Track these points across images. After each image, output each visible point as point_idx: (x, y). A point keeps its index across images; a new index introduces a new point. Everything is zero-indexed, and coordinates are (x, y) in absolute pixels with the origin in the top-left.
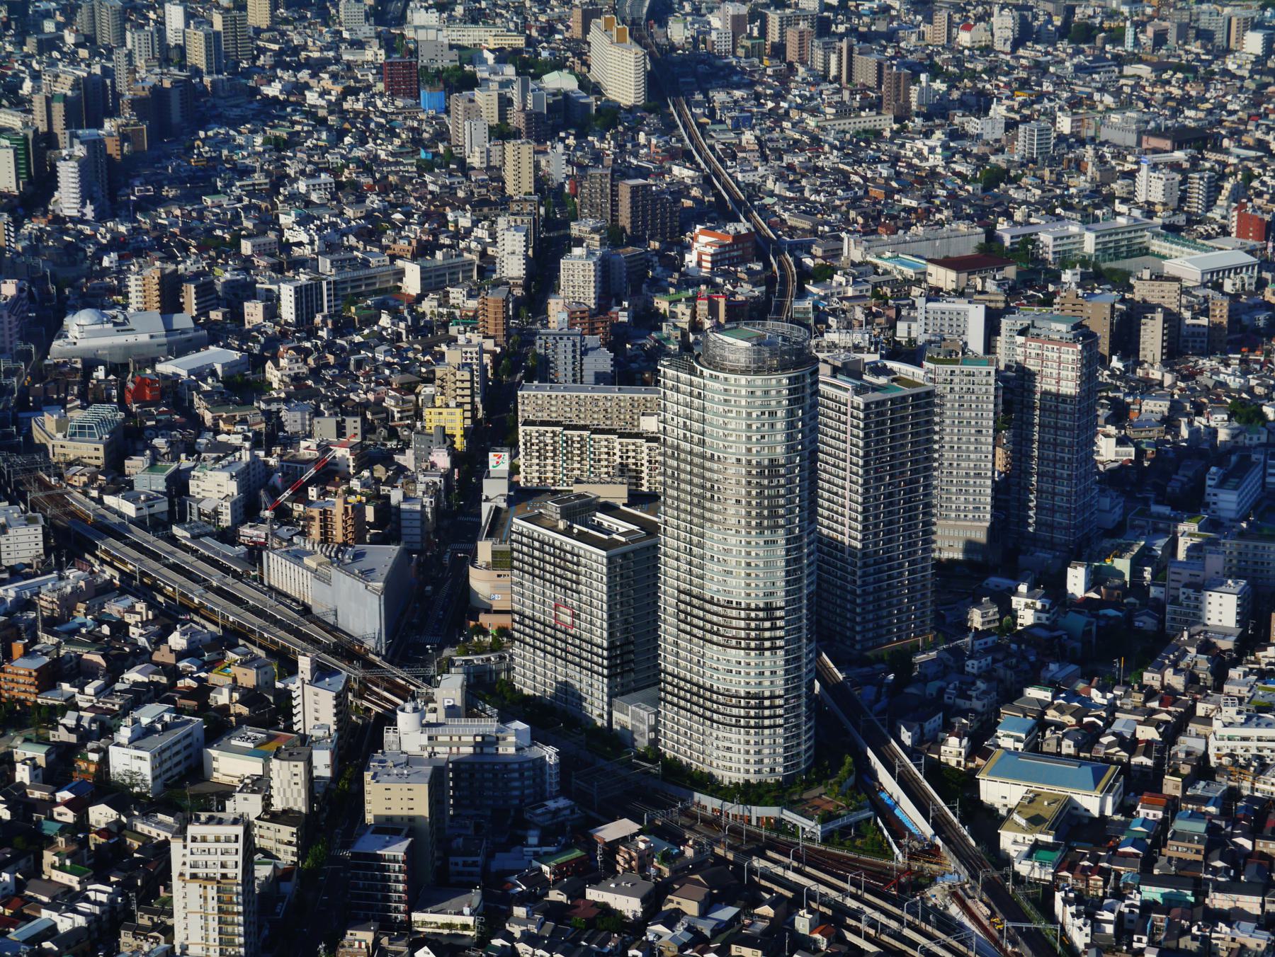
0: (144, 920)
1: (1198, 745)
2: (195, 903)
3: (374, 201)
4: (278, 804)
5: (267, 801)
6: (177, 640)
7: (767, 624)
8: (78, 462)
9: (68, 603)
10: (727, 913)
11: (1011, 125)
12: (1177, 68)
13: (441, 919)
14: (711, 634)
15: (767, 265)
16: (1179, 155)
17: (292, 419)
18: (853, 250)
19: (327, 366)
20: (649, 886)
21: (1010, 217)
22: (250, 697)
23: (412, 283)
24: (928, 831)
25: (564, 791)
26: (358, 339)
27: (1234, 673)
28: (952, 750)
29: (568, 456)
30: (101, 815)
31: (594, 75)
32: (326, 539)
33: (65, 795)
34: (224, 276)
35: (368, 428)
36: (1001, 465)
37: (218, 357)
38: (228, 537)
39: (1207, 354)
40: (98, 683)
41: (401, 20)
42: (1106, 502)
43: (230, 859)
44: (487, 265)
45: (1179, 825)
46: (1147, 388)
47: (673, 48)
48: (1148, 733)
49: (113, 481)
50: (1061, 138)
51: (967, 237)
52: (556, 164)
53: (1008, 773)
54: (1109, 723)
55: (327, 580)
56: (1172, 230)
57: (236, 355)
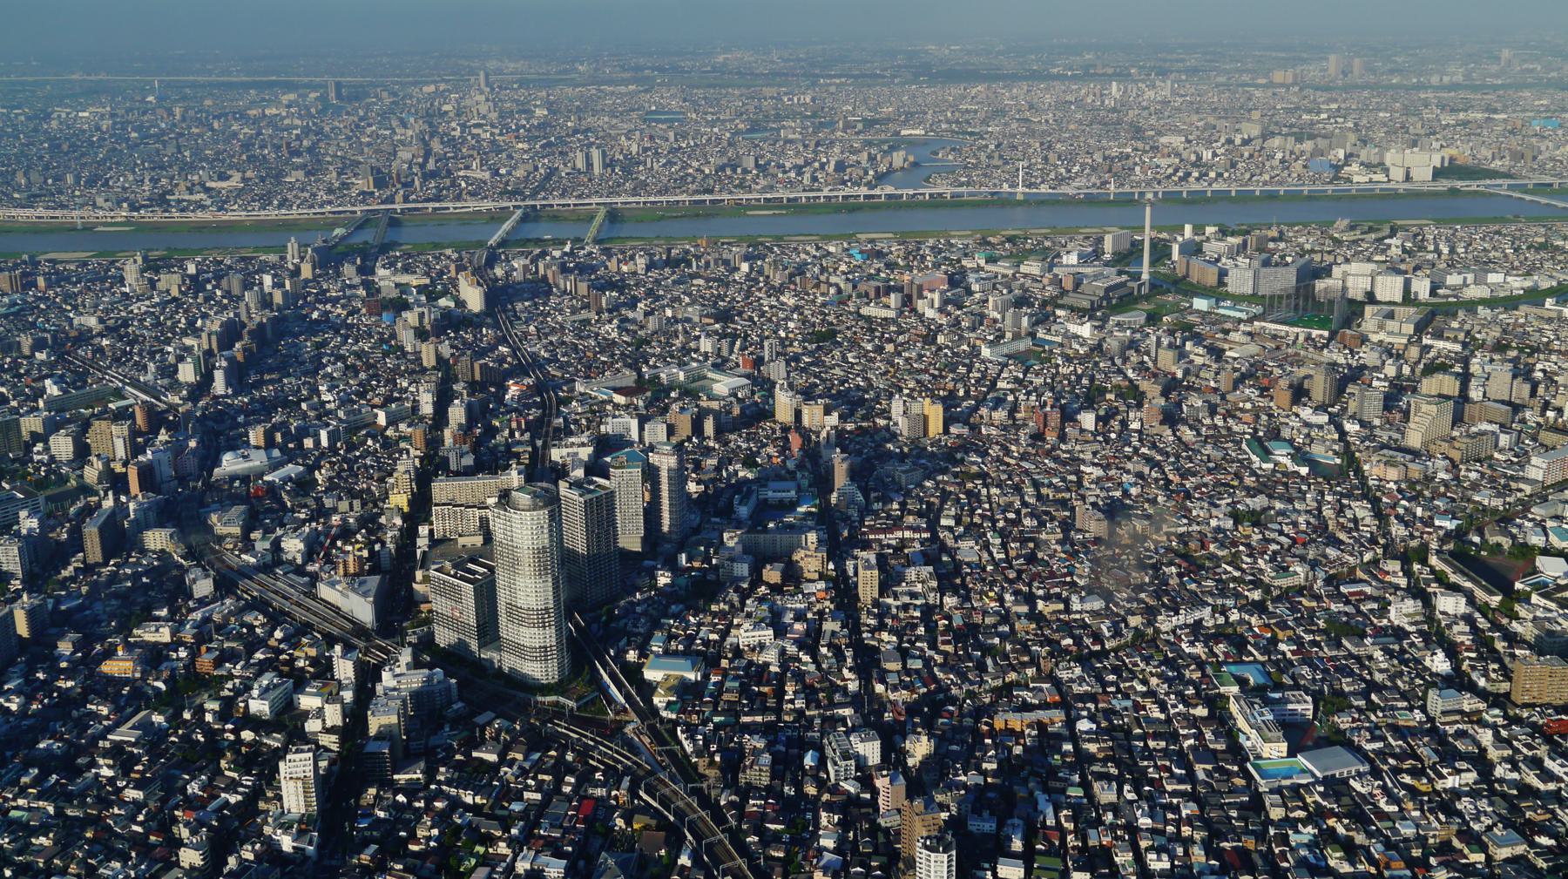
0: (270, 794)
1: (735, 640)
2: (292, 790)
3: (363, 375)
4: (329, 724)
5: (324, 721)
6: (278, 634)
8: (229, 535)
9: (226, 619)
10: (536, 756)
11: (647, 314)
12: (715, 280)
13: (407, 776)
14: (521, 622)
15: (542, 397)
16: (717, 326)
17: (328, 502)
18: (580, 387)
19: (344, 470)
20: (500, 747)
21: (647, 362)
22: (314, 662)
23: (382, 419)
25: (461, 699)
27: (748, 602)
28: (632, 656)
29: (456, 519)
30: (247, 735)
31: (462, 296)
32: (346, 575)
33: (229, 726)
34: (294, 424)
35: (364, 505)
37: (292, 470)
38: (300, 571)
39: (731, 432)
40: (242, 663)
41: (373, 273)
42: (693, 517)
43: (307, 769)
44: (415, 408)
45: (728, 684)
46: (708, 451)
47: (497, 280)
49: (245, 545)
51: (628, 377)
52: (446, 350)
53: (654, 667)
54: (698, 632)
55: (347, 597)
56: (716, 367)
57: (301, 468)
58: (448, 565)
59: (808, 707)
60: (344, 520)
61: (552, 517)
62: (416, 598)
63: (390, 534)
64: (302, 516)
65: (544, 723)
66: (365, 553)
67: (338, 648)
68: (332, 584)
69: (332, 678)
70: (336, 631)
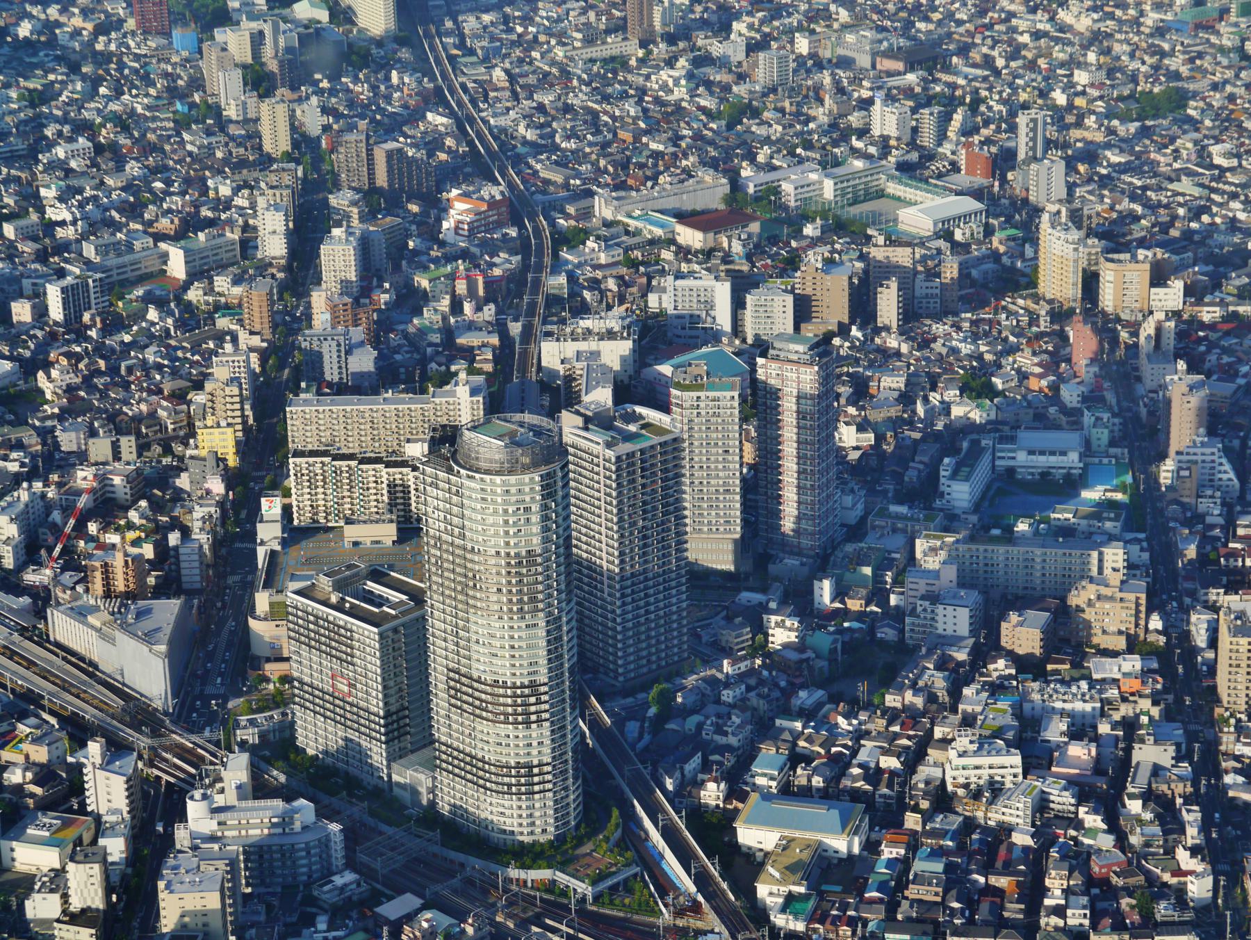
1: (937, 773)
3: (133, 168)
4: (76, 904)
5: (65, 897)
7: (533, 700)
11: (753, 48)
14: (479, 710)
15: (521, 227)
16: (912, 78)
17: (68, 440)
18: (603, 208)
19: (98, 373)
21: (751, 157)
22: (44, 775)
23: (177, 266)
24: (687, 884)
25: (351, 864)
26: (127, 338)
27: (968, 691)
28: (712, 793)
29: (338, 485)
32: (108, 594)
35: (142, 448)
36: (749, 457)
39: (938, 317)
42: (848, 500)
44: (248, 244)
45: (919, 866)
48: (890, 763)
50: (800, 60)
52: (312, 118)
54: (855, 753)
55: (112, 641)
56: (904, 168)
58: (325, 583)
59: (1094, 926)
60: (102, 479)
61: (548, 491)
62: (257, 650)
63: (199, 512)
64: (13, 467)
65: (524, 924)
66: (148, 551)
67: (94, 749)
68: (80, 614)
69: (82, 810)
70: (90, 714)
